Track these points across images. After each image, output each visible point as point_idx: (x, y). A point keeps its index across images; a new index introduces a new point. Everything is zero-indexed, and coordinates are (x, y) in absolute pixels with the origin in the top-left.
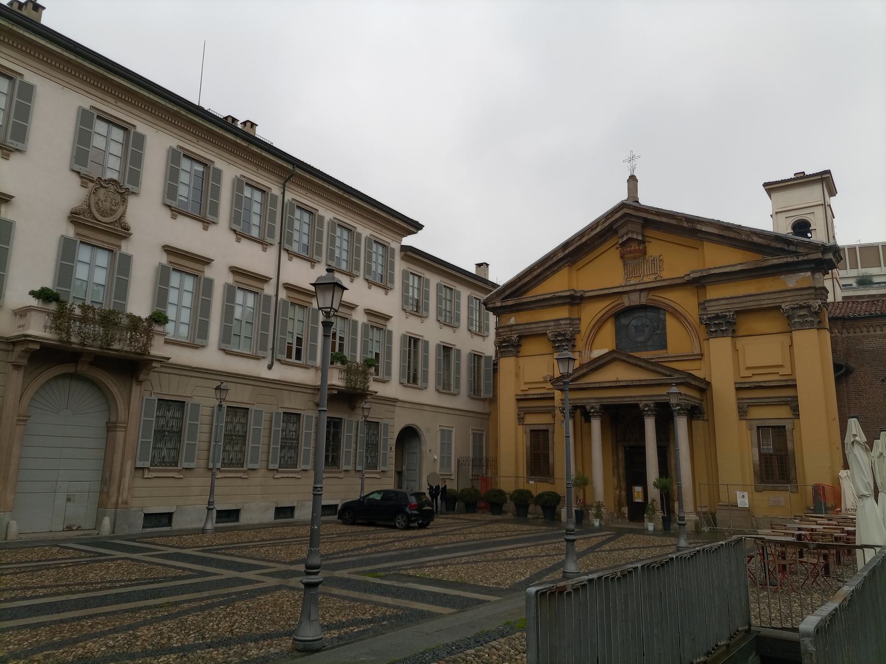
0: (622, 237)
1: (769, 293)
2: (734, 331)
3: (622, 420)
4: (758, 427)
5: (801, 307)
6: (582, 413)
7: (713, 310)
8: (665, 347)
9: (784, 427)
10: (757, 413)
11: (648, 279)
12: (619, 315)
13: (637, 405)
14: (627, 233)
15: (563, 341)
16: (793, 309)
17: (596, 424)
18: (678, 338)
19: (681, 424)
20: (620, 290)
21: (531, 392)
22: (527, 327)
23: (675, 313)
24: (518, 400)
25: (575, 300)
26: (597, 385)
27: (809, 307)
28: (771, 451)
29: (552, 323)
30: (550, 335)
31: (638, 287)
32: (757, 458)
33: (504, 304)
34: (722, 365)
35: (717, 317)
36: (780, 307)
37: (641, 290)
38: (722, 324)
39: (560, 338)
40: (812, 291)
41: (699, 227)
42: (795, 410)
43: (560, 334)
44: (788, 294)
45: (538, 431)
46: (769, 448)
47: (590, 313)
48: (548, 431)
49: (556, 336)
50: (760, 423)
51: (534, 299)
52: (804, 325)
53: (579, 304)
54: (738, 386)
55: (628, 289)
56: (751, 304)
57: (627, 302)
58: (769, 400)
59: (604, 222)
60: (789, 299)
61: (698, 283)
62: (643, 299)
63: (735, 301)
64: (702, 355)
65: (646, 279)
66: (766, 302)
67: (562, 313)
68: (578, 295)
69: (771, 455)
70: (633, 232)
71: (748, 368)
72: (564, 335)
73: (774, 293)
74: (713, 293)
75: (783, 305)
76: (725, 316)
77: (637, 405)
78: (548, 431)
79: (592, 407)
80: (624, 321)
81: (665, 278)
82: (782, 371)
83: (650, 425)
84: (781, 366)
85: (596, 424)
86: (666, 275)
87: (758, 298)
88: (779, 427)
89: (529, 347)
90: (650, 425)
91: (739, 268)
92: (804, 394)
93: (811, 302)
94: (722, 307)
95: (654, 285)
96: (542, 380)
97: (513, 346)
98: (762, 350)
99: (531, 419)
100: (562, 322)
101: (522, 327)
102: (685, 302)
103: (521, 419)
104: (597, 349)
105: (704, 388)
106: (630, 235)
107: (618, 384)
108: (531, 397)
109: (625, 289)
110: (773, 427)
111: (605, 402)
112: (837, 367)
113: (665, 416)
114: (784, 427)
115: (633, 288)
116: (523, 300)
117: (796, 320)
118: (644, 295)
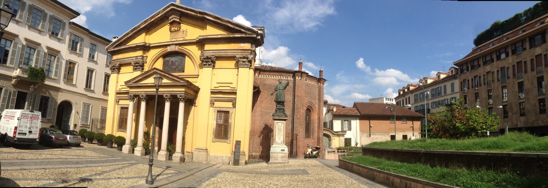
2: (214, 66)
3: (155, 103)
6: (137, 98)
7: (206, 54)
8: (183, 71)
10: (217, 104)
12: (165, 56)
13: (162, 96)
15: (139, 66)
17: (143, 104)
18: (190, 67)
19: (182, 106)
20: (166, 43)
23: (190, 57)
25: (146, 48)
31: (175, 43)
32: (215, 126)
34: (206, 80)
35: (207, 58)
37: (176, 45)
41: (206, 16)
46: (221, 122)
47: (152, 54)
50: (219, 109)
55: (170, 43)
56: (223, 54)
57: (169, 49)
62: (177, 48)
63: (216, 51)
64: (198, 75)
65: (179, 39)
69: (221, 125)
71: (218, 83)
74: (207, 47)
76: (210, 58)
77: (162, 96)
79: (142, 96)
80: (167, 59)
81: (187, 39)
82: (232, 86)
83: (167, 105)
84: (232, 83)
88: (227, 112)
89: (123, 69)
90: (167, 105)
91: (220, 36)
92: (239, 97)
95: (184, 42)
98: (225, 74)
102: (194, 50)
105: (196, 90)
109: (168, 43)
110: (224, 112)
111: (149, 93)
112: (255, 88)
113: (175, 101)
118: (177, 47)
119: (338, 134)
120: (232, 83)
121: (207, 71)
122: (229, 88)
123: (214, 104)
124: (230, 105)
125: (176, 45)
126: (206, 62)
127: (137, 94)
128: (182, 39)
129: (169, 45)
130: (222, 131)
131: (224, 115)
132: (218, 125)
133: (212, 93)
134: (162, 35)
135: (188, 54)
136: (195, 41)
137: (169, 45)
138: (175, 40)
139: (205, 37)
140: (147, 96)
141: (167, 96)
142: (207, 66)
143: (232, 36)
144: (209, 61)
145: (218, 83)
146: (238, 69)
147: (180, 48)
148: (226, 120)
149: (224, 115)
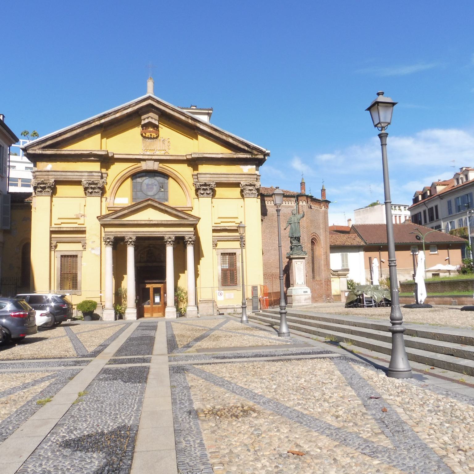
0: (144, 120)
1: (234, 174)
4: (222, 254)
5: (251, 185)
7: (203, 180)
9: (235, 254)
11: (160, 154)
14: (148, 118)
16: (246, 185)
17: (130, 251)
21: (63, 225)
22: (63, 174)
24: (52, 232)
25: (106, 160)
26: (136, 222)
27: (254, 185)
28: (227, 267)
29: (86, 174)
30: (85, 182)
31: (154, 157)
33: (44, 152)
35: (205, 185)
36: (240, 183)
37: (155, 160)
38: (206, 189)
39: (93, 186)
40: (256, 176)
41: (198, 125)
42: (243, 245)
43: (93, 183)
44: (244, 176)
45: (68, 256)
46: (226, 266)
47: (117, 170)
48: (76, 256)
49: (90, 184)
51: (73, 153)
52: (250, 195)
53: (108, 162)
54: (214, 228)
56: (224, 180)
57: (144, 166)
58: (229, 238)
59: (134, 106)
60: (244, 179)
61: (194, 162)
62: (155, 166)
65: (158, 153)
66: (232, 180)
67: (96, 167)
68: (110, 155)
70: (152, 118)
72: (96, 184)
73: (237, 174)
74: (203, 168)
75: (242, 183)
76: (209, 185)
78: (76, 256)
83: (170, 251)
84: (237, 218)
85: (130, 251)
86: (171, 152)
87: (228, 176)
90: (170, 251)
91: (220, 156)
93: (256, 183)
94: (208, 179)
96: (75, 217)
97: (49, 187)
99: (62, 247)
100: (94, 174)
101: (58, 173)
103: (53, 247)
104: (120, 197)
106: (150, 120)
107: (151, 223)
108: (65, 229)
111: (140, 235)
114: (235, 254)
115: (150, 157)
116: (63, 152)
117: (247, 192)
119: (337, 274)
120: (237, 218)
121: (206, 201)
122: (233, 224)
123: (216, 245)
124: (237, 244)
125: (155, 160)
126: (204, 189)
127: (119, 235)
128: (162, 153)
129: (144, 160)
130: (229, 277)
131: (230, 256)
132: (224, 271)
133: (214, 231)
134: (127, 143)
135: (173, 176)
136: (185, 158)
137: (144, 160)
138: (151, 153)
139: (200, 156)
140: (138, 238)
141: (170, 238)
142: (205, 195)
143: (235, 156)
144: (207, 189)
145: (219, 218)
146: (244, 199)
147: (161, 165)
148: (233, 264)
149: (230, 256)
